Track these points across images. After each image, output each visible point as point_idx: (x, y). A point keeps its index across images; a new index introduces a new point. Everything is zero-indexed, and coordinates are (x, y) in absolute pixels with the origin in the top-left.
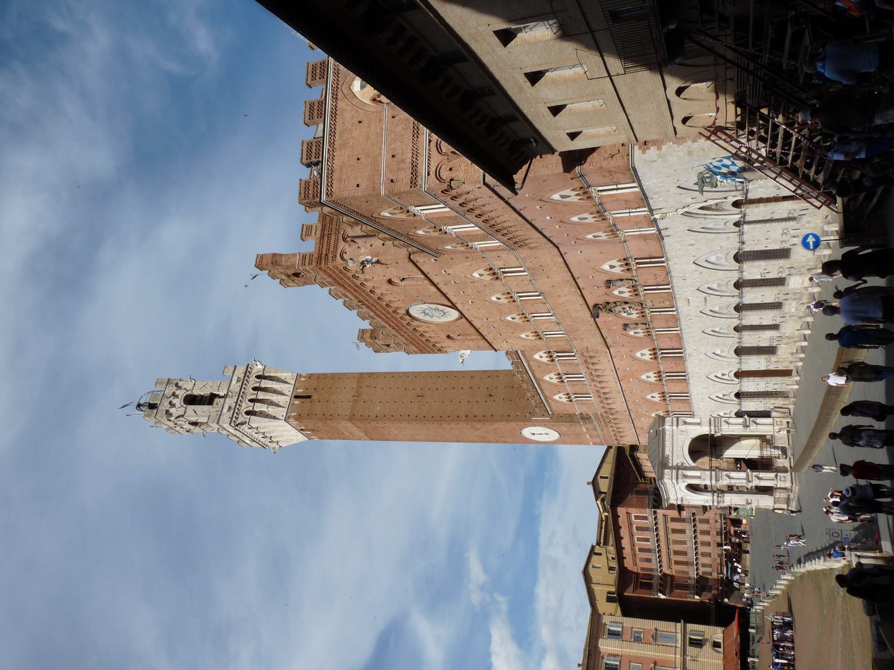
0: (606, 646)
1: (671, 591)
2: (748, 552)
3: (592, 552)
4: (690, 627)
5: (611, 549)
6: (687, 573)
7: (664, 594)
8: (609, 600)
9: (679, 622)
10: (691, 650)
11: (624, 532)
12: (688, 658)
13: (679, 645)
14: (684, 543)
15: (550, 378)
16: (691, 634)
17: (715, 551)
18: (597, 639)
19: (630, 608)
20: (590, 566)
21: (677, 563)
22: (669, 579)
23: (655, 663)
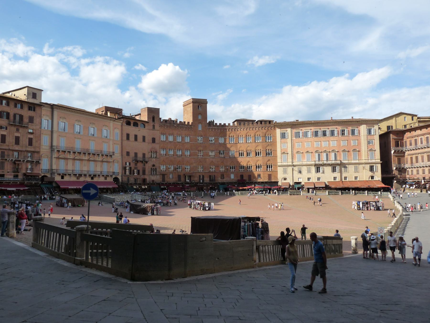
0: (363, 129)
1: (396, 156)
2: (421, 192)
3: (413, 116)
4: (379, 166)
5: (417, 125)
6: (407, 163)
7: (394, 153)
8: (388, 127)
9: (381, 161)
10: (368, 167)
11: (424, 131)
12: (364, 166)
13: (369, 161)
14: (423, 161)
15: (171, 138)
16: (375, 166)
17: (420, 176)
18: (366, 124)
19: (384, 138)
20: (405, 116)
21: (411, 158)
22: (403, 155)
23: (359, 151)
